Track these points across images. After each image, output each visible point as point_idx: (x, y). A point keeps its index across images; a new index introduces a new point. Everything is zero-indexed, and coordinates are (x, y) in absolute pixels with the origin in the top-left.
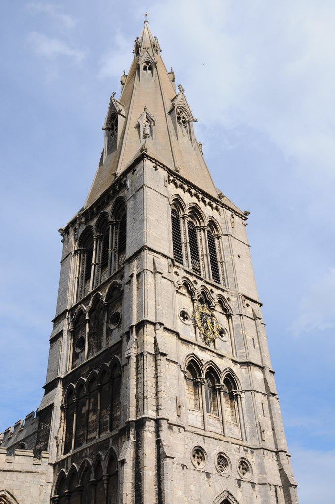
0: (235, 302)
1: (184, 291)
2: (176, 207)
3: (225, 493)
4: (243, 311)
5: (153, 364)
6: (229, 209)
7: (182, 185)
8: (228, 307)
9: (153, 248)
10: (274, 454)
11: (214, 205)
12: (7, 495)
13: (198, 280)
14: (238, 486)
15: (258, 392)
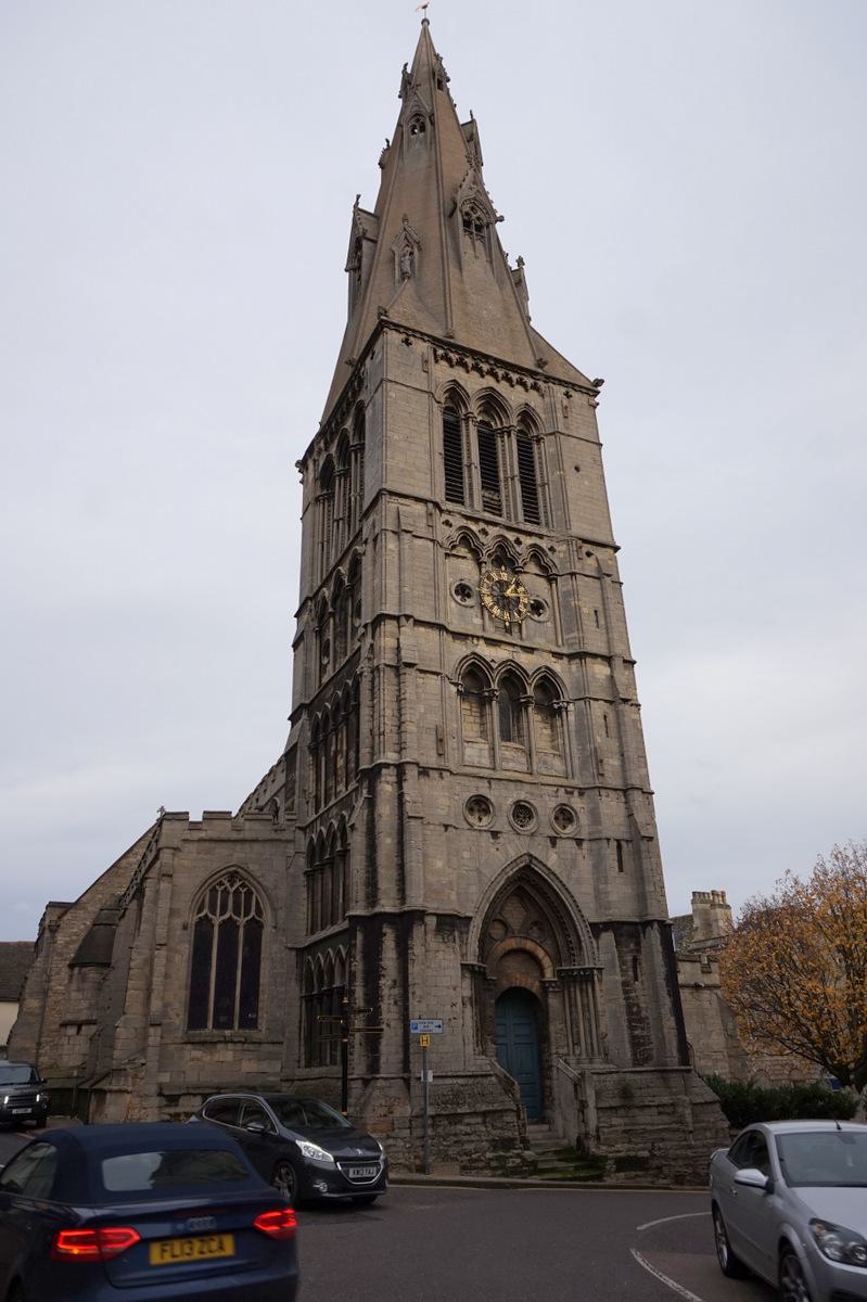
0: (564, 552)
1: (463, 551)
2: (453, 402)
3: (527, 858)
4: (578, 565)
5: (395, 681)
6: (561, 382)
7: (462, 359)
8: (551, 564)
9: (400, 490)
10: (621, 793)
11: (529, 381)
12: (239, 870)
13: (490, 527)
14: (549, 844)
15: (597, 700)
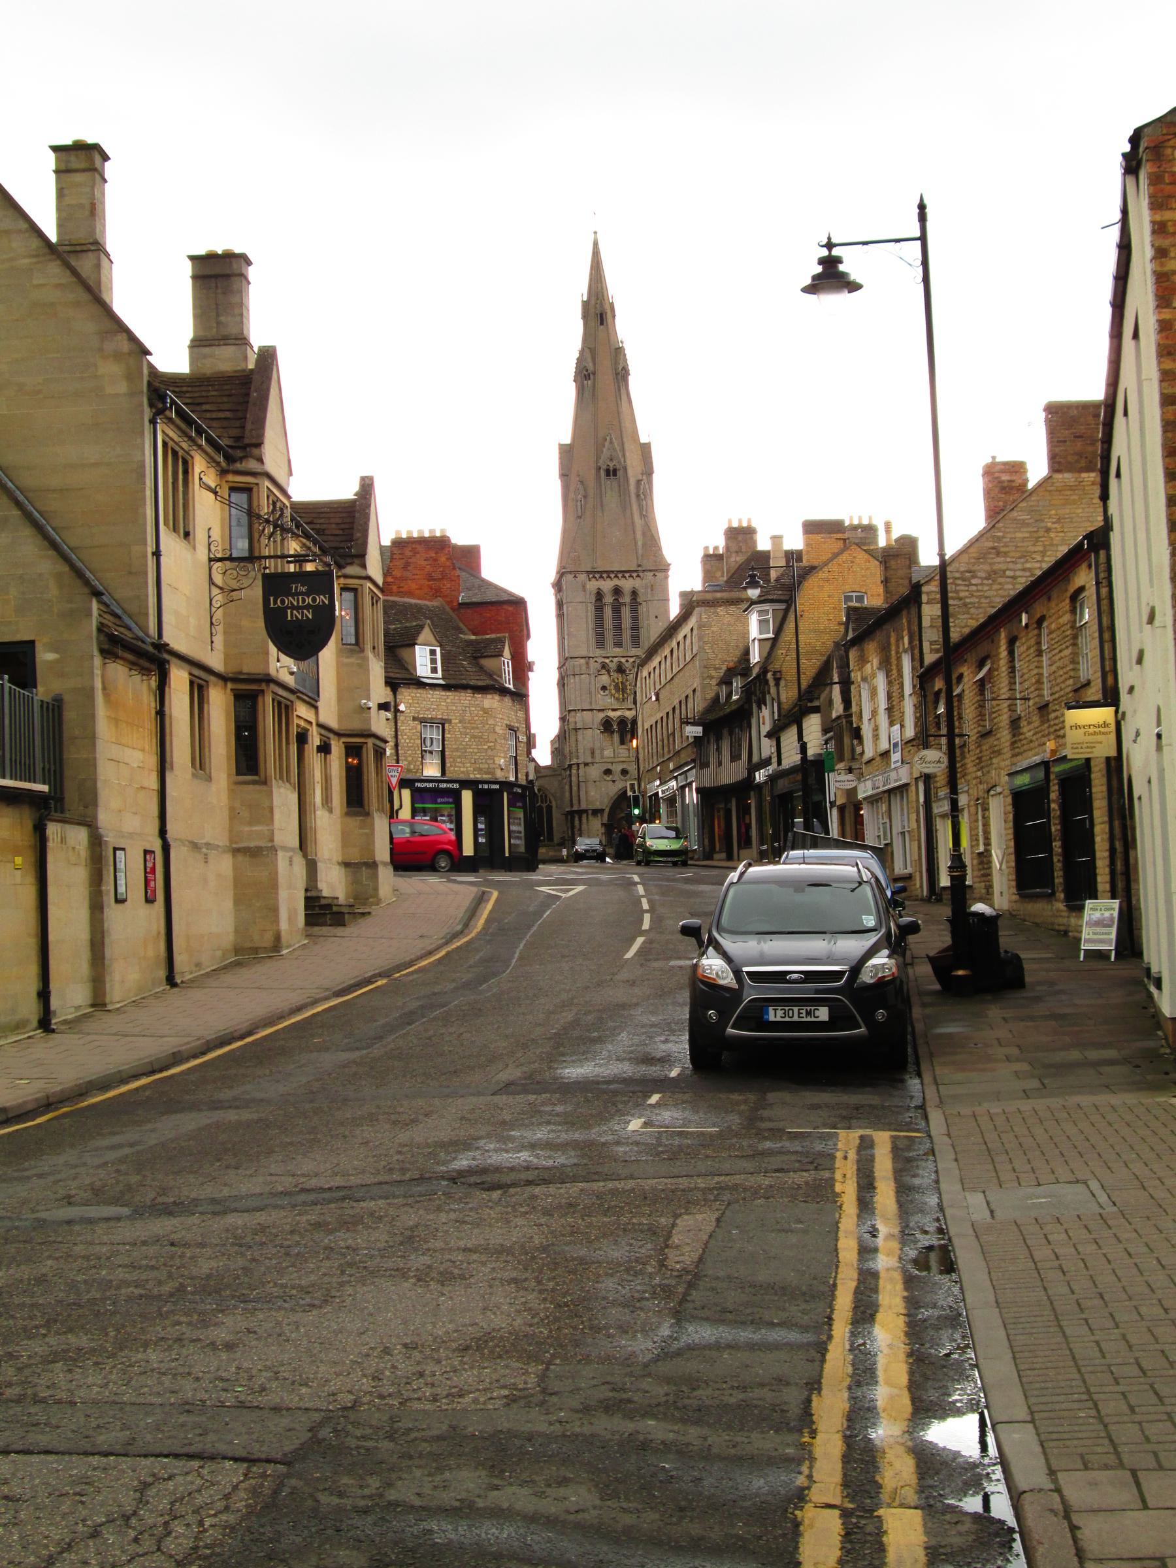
1: (604, 671)
